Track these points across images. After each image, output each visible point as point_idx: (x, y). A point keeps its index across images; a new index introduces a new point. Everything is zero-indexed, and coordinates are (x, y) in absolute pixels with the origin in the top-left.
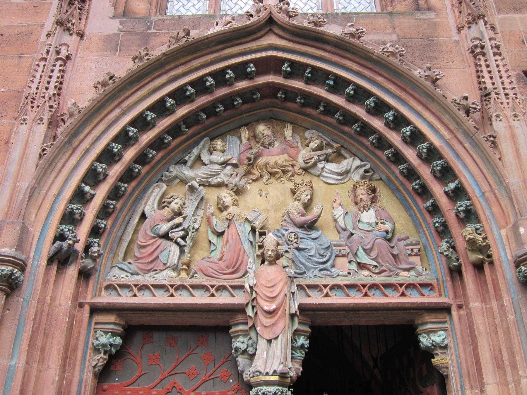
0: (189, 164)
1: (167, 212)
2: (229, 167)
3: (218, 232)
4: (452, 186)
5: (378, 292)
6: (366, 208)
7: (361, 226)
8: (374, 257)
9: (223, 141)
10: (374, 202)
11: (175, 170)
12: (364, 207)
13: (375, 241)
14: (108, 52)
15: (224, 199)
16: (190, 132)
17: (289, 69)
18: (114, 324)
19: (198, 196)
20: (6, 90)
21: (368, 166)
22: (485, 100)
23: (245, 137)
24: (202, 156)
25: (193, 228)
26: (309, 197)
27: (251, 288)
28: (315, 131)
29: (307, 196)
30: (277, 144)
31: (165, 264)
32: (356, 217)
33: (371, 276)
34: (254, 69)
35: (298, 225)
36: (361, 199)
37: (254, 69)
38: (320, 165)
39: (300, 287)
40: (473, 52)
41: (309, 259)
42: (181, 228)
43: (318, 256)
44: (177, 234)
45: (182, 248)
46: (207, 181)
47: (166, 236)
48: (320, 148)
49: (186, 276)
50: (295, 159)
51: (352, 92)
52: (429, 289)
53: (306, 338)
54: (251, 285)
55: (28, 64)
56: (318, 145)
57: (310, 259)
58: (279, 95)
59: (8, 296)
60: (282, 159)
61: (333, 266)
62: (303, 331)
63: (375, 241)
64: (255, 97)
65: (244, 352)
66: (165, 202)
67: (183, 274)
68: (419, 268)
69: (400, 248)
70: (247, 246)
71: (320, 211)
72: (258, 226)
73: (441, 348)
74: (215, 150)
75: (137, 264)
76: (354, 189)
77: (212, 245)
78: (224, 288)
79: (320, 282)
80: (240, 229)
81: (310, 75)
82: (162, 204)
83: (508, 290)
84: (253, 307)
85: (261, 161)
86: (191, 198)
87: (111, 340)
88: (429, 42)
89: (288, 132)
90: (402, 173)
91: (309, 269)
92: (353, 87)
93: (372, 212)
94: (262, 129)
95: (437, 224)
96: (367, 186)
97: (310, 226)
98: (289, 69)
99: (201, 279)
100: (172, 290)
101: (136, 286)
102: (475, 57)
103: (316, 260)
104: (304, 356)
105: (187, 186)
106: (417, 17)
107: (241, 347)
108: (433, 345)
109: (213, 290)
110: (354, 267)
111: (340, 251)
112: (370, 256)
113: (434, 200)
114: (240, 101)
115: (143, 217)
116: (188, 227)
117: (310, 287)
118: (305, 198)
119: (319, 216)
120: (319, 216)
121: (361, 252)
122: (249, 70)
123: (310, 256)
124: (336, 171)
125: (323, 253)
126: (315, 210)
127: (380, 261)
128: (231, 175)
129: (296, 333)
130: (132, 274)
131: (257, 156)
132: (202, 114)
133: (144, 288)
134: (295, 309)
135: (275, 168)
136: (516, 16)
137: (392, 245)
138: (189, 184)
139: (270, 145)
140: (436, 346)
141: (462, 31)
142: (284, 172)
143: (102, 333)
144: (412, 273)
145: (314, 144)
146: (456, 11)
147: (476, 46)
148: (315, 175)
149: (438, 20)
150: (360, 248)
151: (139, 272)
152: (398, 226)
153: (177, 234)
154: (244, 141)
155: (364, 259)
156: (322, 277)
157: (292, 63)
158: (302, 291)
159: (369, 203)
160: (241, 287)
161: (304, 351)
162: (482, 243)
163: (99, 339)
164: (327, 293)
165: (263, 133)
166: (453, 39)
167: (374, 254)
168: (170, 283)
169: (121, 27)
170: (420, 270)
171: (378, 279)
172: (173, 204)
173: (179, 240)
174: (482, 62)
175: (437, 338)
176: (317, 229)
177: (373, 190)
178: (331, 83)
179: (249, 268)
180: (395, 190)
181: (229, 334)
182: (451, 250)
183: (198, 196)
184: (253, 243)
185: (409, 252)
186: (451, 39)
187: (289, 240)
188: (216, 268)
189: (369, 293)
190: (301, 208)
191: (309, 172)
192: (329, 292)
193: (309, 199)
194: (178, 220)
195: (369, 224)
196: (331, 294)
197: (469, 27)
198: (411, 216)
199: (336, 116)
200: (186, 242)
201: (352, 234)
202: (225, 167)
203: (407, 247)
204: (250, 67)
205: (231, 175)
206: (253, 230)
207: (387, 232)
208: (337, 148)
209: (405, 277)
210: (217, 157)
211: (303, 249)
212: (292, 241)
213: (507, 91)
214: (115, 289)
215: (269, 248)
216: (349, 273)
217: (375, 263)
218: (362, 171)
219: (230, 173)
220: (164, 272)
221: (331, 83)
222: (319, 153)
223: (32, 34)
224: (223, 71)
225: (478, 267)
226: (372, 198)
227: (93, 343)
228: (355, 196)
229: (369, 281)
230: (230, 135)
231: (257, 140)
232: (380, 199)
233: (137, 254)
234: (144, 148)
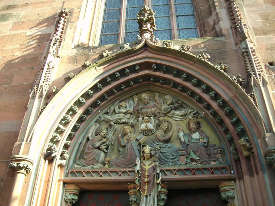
0: (110, 114)
1: (98, 137)
2: (128, 115)
3: (123, 146)
4: (234, 119)
5: (200, 172)
6: (194, 132)
7: (192, 141)
8: (198, 155)
10: (198, 129)
12: (193, 131)
13: (198, 148)
14: (71, 64)
15: (126, 130)
16: (109, 98)
17: (155, 67)
18: (74, 189)
19: (113, 129)
20: (26, 84)
21: (195, 112)
22: (249, 77)
23: (136, 100)
24: (115, 110)
25: (111, 144)
26: (167, 127)
27: (138, 171)
28: (169, 96)
29: (166, 127)
31: (98, 161)
32: (190, 137)
33: (197, 165)
34: (138, 68)
35: (161, 141)
36: (192, 127)
37: (138, 68)
38: (172, 112)
39: (162, 171)
40: (243, 55)
42: (105, 144)
43: (171, 155)
44: (103, 147)
45: (106, 153)
46: (118, 122)
47: (98, 148)
48: (172, 104)
49: (108, 167)
51: (186, 77)
52: (225, 170)
53: (165, 195)
54: (138, 170)
55: (36, 71)
56: (171, 102)
57: (167, 157)
58: (151, 79)
62: (163, 192)
63: (198, 148)
64: (140, 81)
66: (98, 132)
68: (221, 160)
69: (212, 150)
71: (172, 134)
73: (231, 198)
74: (122, 107)
75: (85, 162)
76: (189, 123)
77: (120, 152)
78: (126, 172)
79: (171, 168)
81: (165, 69)
84: (139, 180)
86: (110, 130)
87: (73, 197)
88: (222, 51)
89: (157, 97)
90: (211, 113)
91: (166, 162)
92: (186, 74)
93: (197, 133)
94: (144, 96)
95: (228, 138)
96: (195, 121)
97: (167, 141)
98: (155, 67)
100: (101, 174)
101: (84, 172)
102: (244, 57)
103: (170, 157)
104: (164, 204)
105: (108, 124)
106: (216, 40)
107: (134, 200)
108: (227, 197)
109: (120, 173)
110: (189, 161)
111: (182, 153)
112: (196, 155)
113: (227, 127)
114: (133, 83)
116: (109, 144)
117: (167, 170)
119: (171, 136)
120: (171, 136)
121: (192, 153)
122: (136, 68)
123: (167, 156)
124: (180, 114)
125: (174, 154)
127: (201, 157)
128: (129, 118)
129: (160, 193)
130: (82, 166)
131: (142, 109)
132: (115, 90)
133: (88, 172)
135: (150, 114)
136: (264, 36)
137: (207, 150)
138: (109, 123)
139: (148, 103)
140: (228, 197)
141: (238, 45)
143: (69, 194)
144: (217, 162)
145: (168, 103)
146: (235, 35)
147: (244, 52)
148: (170, 117)
149: (226, 40)
150: (191, 151)
151: (86, 165)
152: (211, 140)
153: (103, 147)
154: (136, 102)
155: (194, 157)
156: (173, 166)
157: (157, 64)
158: (163, 173)
159: (196, 129)
160: (134, 171)
161: (165, 201)
162: (249, 146)
163: (67, 196)
164: (175, 173)
165: (144, 98)
166: (234, 49)
167: (198, 154)
168: (100, 170)
169: (77, 52)
170: (221, 161)
171: (200, 166)
172: (101, 133)
173: (105, 150)
174: (247, 60)
175: (229, 194)
176: (171, 143)
177: (198, 123)
178: (176, 73)
179: (137, 162)
180: (208, 123)
181: (128, 194)
182: (235, 150)
183: (113, 129)
184: (140, 150)
185: (216, 152)
186: (233, 49)
187: (156, 148)
188: (122, 162)
189: (196, 173)
190: (163, 132)
191: (166, 115)
192: (176, 173)
193: (166, 129)
194: (104, 140)
196: (177, 174)
197: (241, 43)
198: (216, 135)
199: (179, 88)
200: (108, 151)
201: (188, 145)
202: (127, 114)
203: (215, 150)
204: (137, 67)
205: (129, 118)
206: (140, 144)
207: (205, 143)
208: (180, 103)
210: (123, 110)
211: (164, 153)
212: (157, 149)
213: (259, 73)
214: (74, 173)
215: (146, 152)
216: (186, 164)
217: (199, 158)
219: (129, 117)
220: (98, 165)
221: (176, 73)
223: (38, 58)
224: (124, 70)
225: (248, 158)
226: (198, 127)
227: (65, 199)
228: (189, 126)
230: (129, 99)
231: (142, 101)
232: (202, 127)
233: (85, 157)
234: (88, 107)
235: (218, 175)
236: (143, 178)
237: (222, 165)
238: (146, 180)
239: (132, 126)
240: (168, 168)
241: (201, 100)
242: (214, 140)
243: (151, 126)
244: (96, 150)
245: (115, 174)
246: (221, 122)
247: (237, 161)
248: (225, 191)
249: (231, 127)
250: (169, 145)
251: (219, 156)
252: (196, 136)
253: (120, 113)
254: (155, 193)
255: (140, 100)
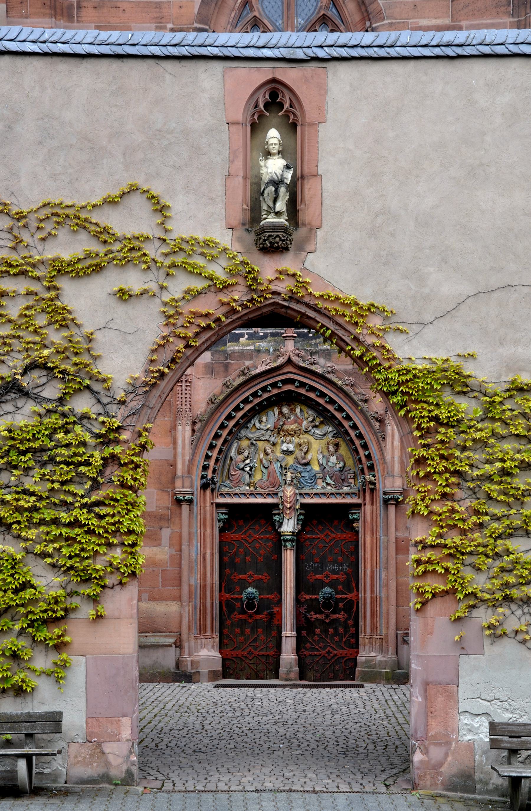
0: (250, 428)
1: (241, 457)
6: (332, 455)
9: (267, 416)
11: (243, 432)
14: (208, 376)
30: (292, 417)
39: (300, 494)
41: (306, 482)
44: (248, 469)
45: (250, 475)
47: (243, 469)
50: (301, 426)
59: (189, 505)
60: (293, 427)
61: (316, 484)
65: (279, 521)
67: (252, 489)
68: (352, 485)
70: (278, 474)
72: (283, 465)
80: (275, 466)
82: (239, 453)
83: (379, 503)
85: (286, 427)
93: (335, 457)
94: (285, 410)
99: (259, 490)
110: (324, 484)
115: (231, 459)
117: (305, 494)
118: (305, 450)
121: (328, 478)
126: (309, 457)
131: (282, 426)
134: (298, 507)
142: (295, 433)
145: (310, 419)
154: (276, 415)
155: (329, 481)
167: (333, 479)
171: (334, 491)
175: (355, 517)
177: (337, 446)
194: (247, 461)
195: (333, 463)
206: (281, 466)
209: (346, 489)
217: (333, 483)
218: (332, 434)
222: (312, 424)
225: (372, 490)
229: (330, 492)
235: (348, 500)
236: (286, 504)
237: (353, 491)
238: (288, 506)
239: (274, 444)
240: (307, 491)
241: (341, 425)
242: (350, 462)
243: (291, 447)
244: (240, 472)
245: (260, 496)
246: (356, 451)
247: (364, 491)
248: (352, 514)
249: (363, 459)
250: (308, 468)
251: (352, 481)
252: (333, 459)
253: (260, 429)
254: (294, 515)
255: (281, 413)
